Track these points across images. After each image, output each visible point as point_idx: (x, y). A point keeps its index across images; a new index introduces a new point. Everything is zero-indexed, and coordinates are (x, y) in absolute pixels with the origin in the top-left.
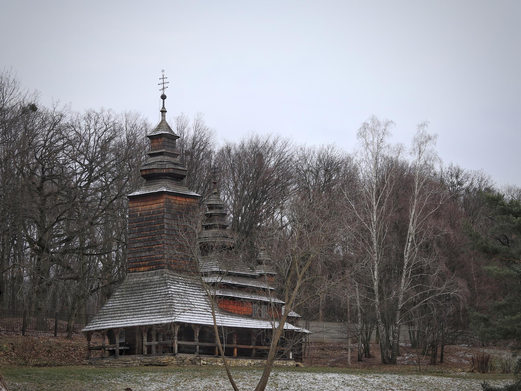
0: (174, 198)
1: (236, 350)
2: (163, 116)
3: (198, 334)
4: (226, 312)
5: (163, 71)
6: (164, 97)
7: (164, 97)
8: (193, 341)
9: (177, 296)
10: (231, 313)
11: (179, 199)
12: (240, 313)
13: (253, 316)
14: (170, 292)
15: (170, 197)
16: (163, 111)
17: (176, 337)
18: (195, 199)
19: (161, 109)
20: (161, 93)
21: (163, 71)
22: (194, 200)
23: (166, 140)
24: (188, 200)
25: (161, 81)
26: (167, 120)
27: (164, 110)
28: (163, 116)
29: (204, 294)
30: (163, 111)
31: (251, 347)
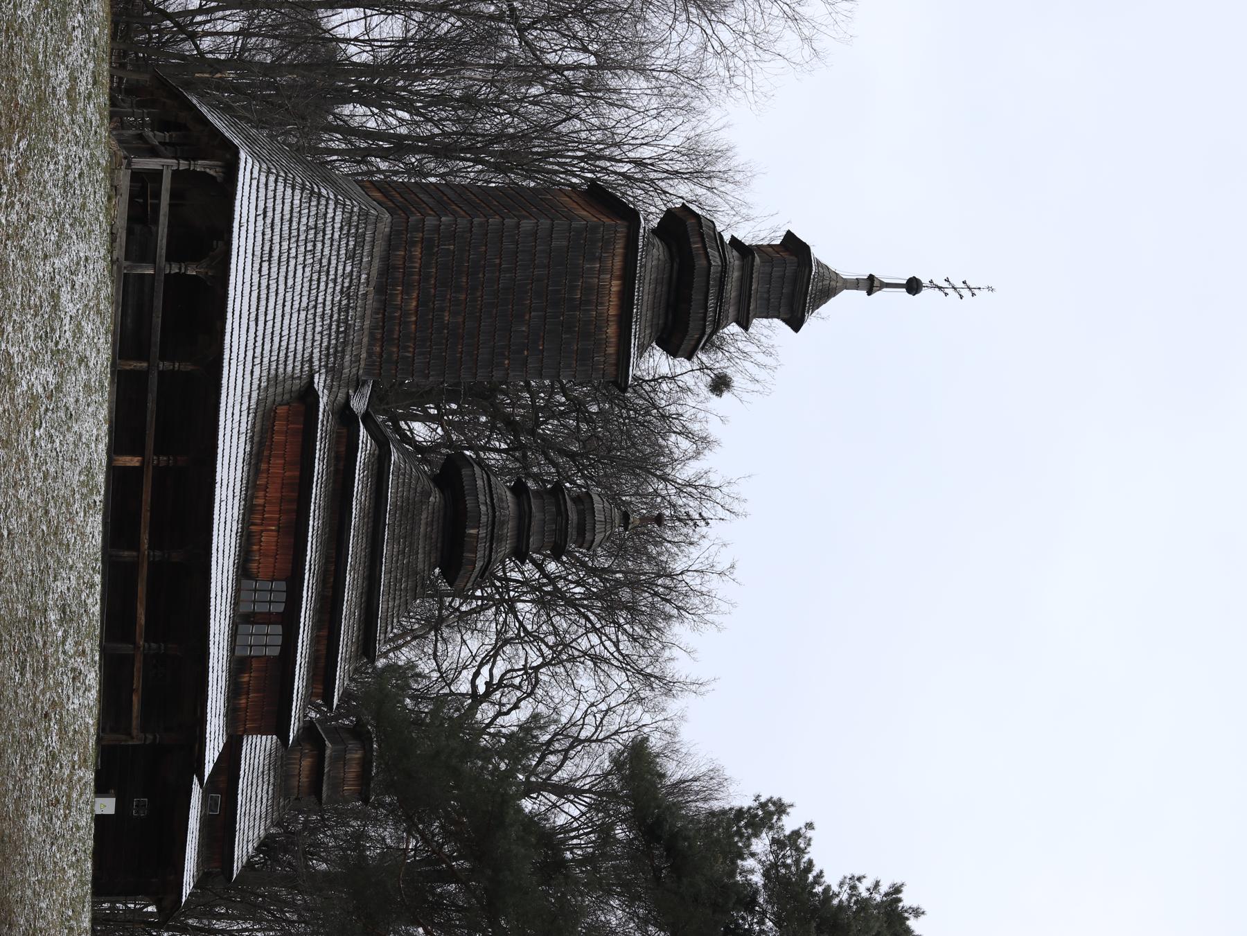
0: (618, 263)
1: (134, 461)
2: (855, 284)
3: (191, 272)
4: (261, 443)
5: (990, 289)
6: (913, 286)
7: (913, 286)
8: (170, 258)
9: (311, 223)
10: (259, 461)
11: (615, 286)
12: (257, 518)
13: (246, 583)
14: (324, 192)
15: (619, 249)
16: (871, 285)
17: (183, 165)
18: (617, 365)
19: (882, 275)
20: (925, 281)
21: (990, 289)
22: (612, 360)
23: (790, 270)
24: (612, 330)
25: (959, 284)
26: (845, 296)
27: (876, 283)
28: (855, 284)
29: (316, 363)
30: (871, 285)
31: (145, 539)
